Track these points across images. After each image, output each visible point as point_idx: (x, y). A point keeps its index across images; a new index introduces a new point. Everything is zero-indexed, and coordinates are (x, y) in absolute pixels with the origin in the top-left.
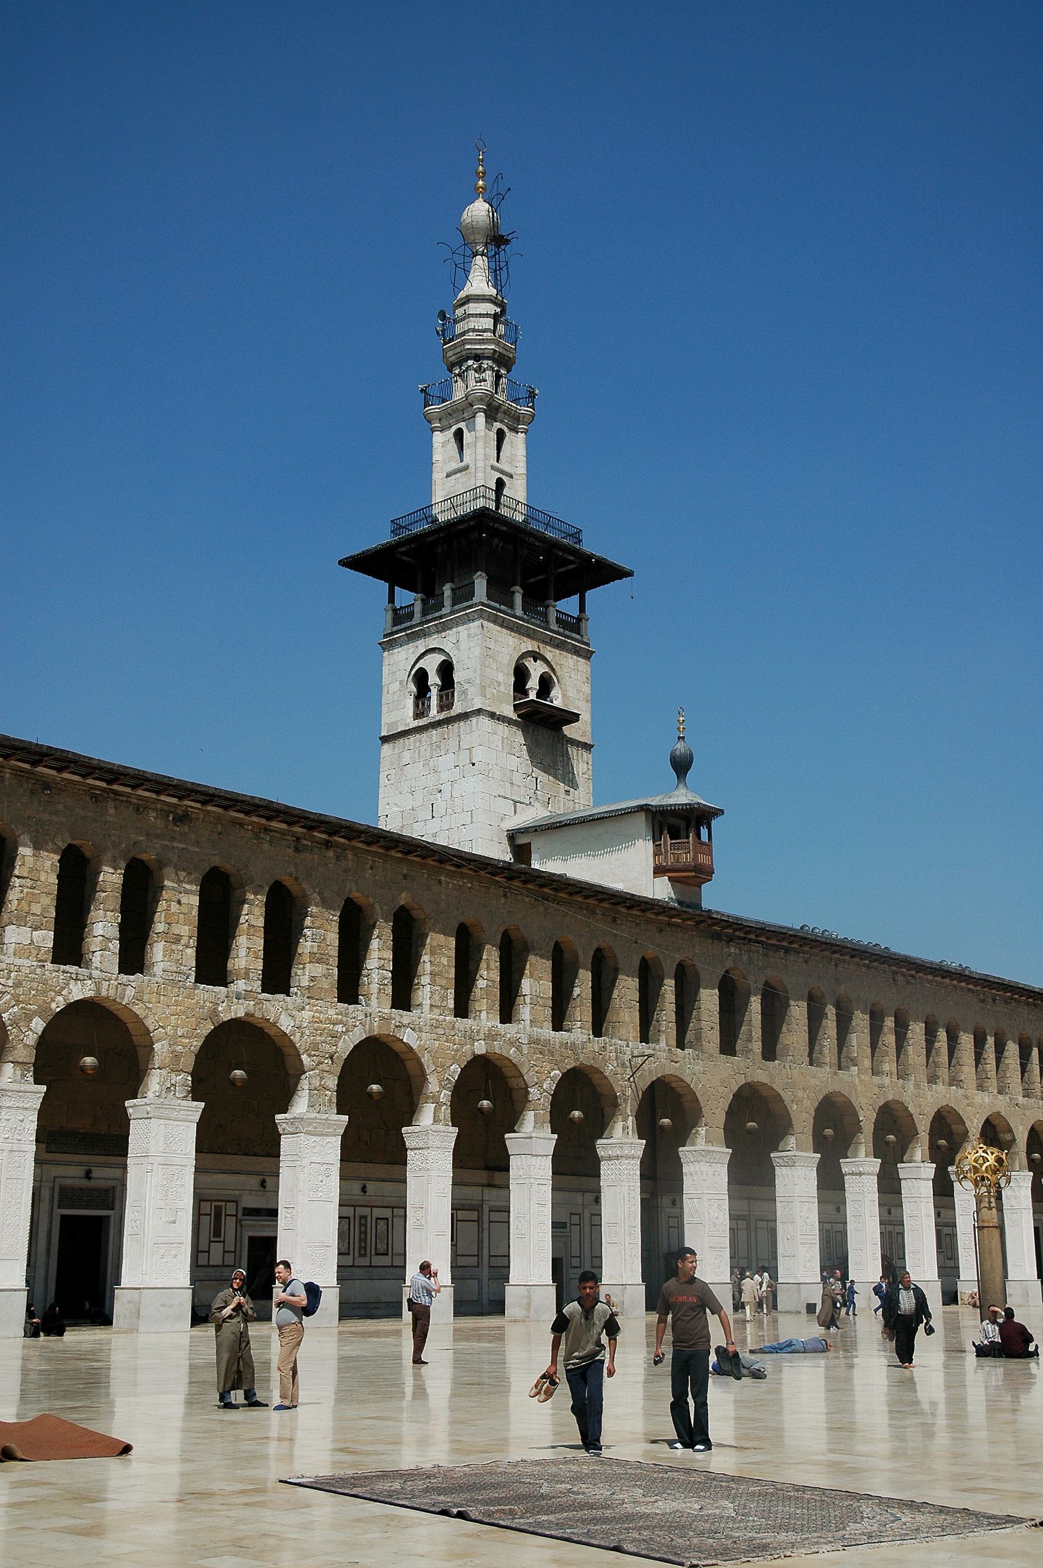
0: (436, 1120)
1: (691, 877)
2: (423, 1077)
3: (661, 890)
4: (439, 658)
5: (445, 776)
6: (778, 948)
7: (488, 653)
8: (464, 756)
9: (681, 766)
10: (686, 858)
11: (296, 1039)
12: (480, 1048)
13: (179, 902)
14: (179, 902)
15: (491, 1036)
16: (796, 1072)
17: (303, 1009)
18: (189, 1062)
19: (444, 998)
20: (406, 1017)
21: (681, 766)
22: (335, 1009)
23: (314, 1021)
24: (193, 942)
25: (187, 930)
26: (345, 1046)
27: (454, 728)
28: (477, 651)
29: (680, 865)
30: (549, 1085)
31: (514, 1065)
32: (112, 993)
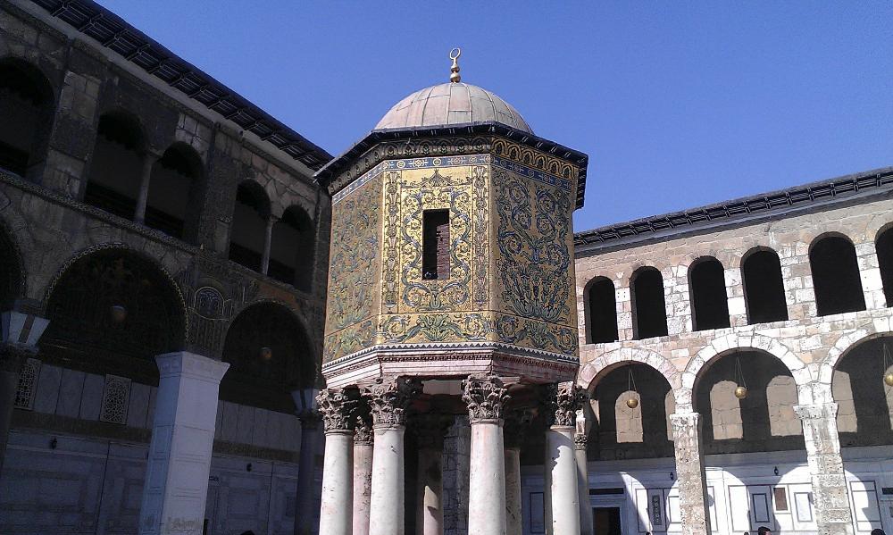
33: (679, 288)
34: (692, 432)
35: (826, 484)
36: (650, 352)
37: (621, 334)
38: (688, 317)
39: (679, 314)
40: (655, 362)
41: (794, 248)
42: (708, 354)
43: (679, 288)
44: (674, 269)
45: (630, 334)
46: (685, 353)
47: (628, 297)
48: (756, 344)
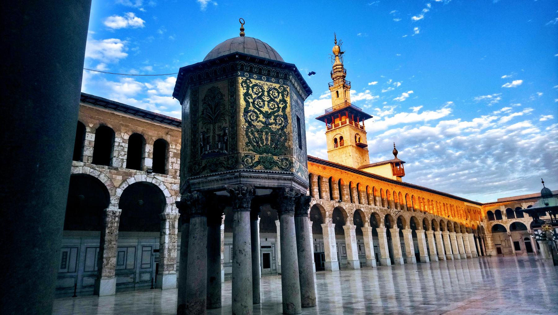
2: (365, 217)
3: (395, 178)
4: (340, 135)
5: (343, 159)
7: (351, 134)
8: (348, 155)
9: (395, 153)
12: (373, 211)
15: (374, 209)
18: (331, 216)
20: (361, 205)
21: (395, 153)
23: (348, 207)
25: (328, 190)
26: (353, 211)
27: (345, 149)
28: (349, 134)
30: (384, 218)
33: (123, 144)
34: (117, 219)
35: (170, 248)
36: (102, 174)
37: (85, 159)
38: (125, 160)
39: (121, 157)
40: (103, 179)
41: (176, 145)
42: (132, 181)
43: (123, 144)
44: (122, 134)
45: (91, 160)
46: (120, 178)
47: (93, 139)
48: (154, 182)
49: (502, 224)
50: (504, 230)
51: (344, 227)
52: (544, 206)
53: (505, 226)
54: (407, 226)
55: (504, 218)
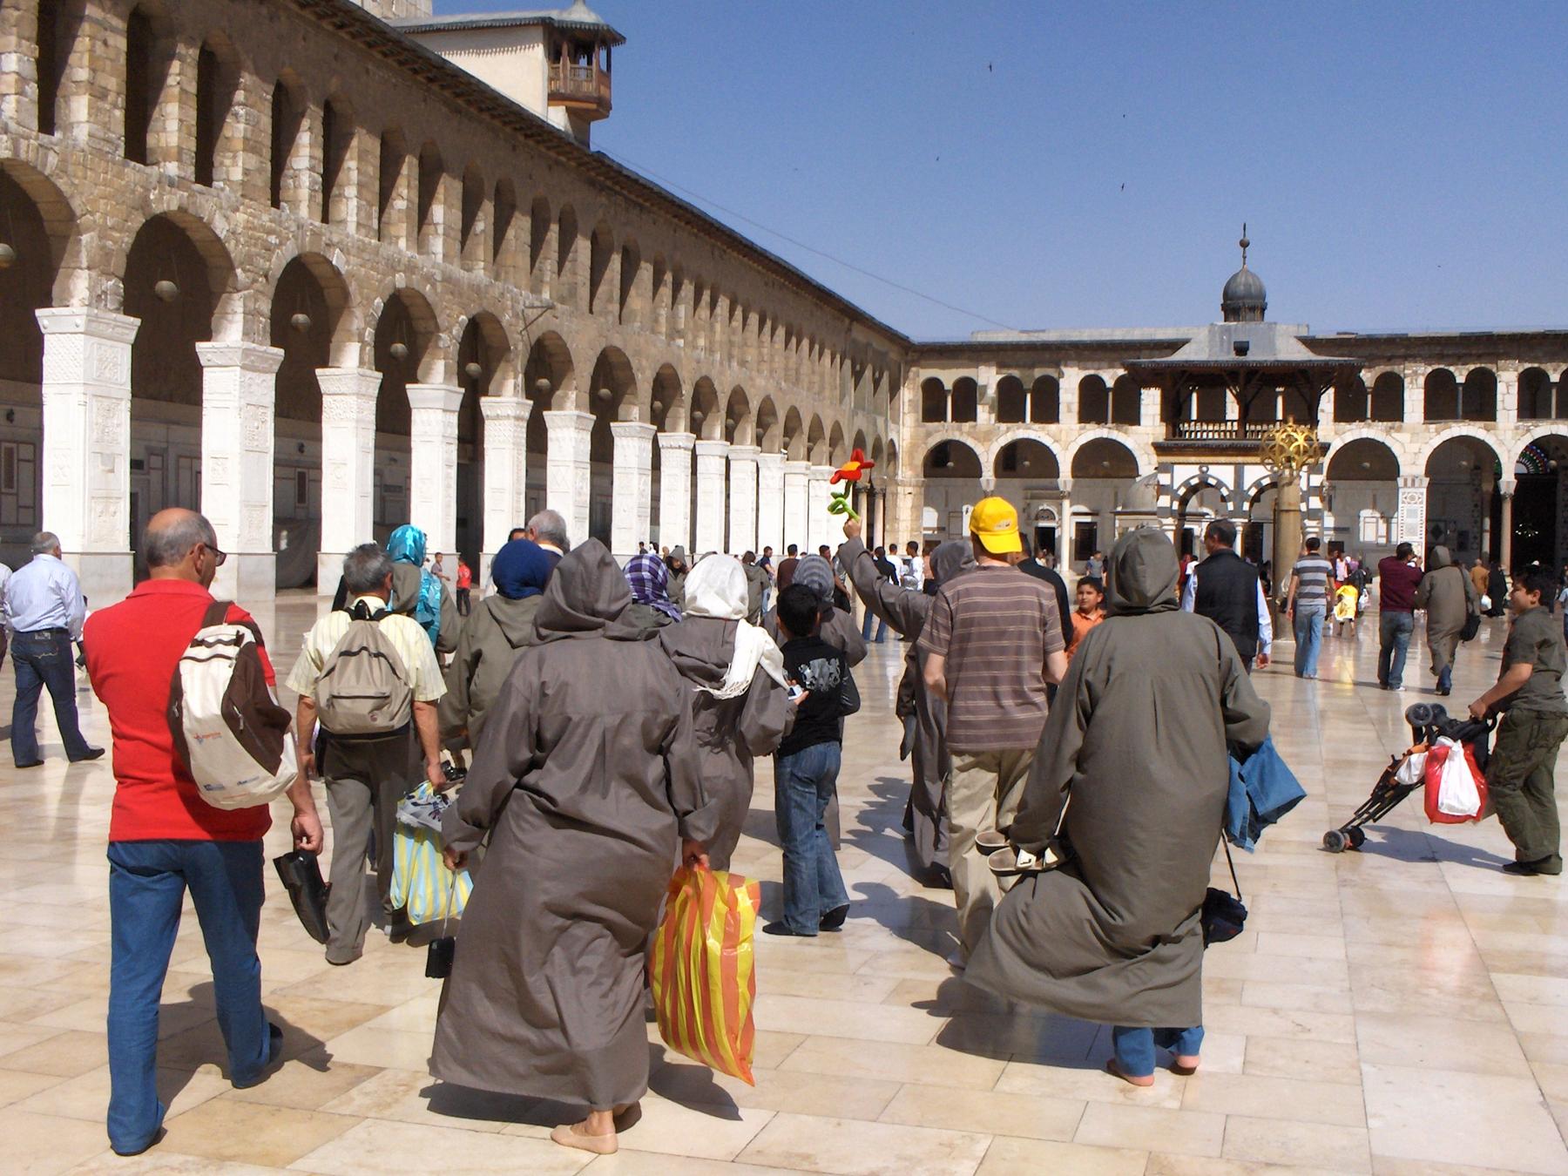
0: (362, 363)
1: (589, 109)
6: (636, 204)
10: (589, 88)
11: (231, 246)
12: (400, 280)
13: (105, 43)
14: (105, 43)
15: (411, 268)
16: (642, 340)
17: (237, 210)
18: (119, 264)
19: (370, 217)
22: (266, 217)
24: (121, 101)
29: (580, 95)
30: (457, 331)
31: (428, 305)
32: (31, 156)
49: (970, 442)
50: (971, 466)
51: (201, 347)
52: (1231, 357)
53: (979, 449)
54: (573, 395)
55: (984, 415)
